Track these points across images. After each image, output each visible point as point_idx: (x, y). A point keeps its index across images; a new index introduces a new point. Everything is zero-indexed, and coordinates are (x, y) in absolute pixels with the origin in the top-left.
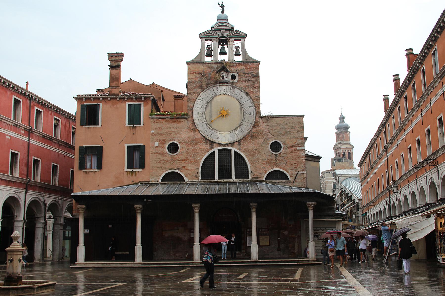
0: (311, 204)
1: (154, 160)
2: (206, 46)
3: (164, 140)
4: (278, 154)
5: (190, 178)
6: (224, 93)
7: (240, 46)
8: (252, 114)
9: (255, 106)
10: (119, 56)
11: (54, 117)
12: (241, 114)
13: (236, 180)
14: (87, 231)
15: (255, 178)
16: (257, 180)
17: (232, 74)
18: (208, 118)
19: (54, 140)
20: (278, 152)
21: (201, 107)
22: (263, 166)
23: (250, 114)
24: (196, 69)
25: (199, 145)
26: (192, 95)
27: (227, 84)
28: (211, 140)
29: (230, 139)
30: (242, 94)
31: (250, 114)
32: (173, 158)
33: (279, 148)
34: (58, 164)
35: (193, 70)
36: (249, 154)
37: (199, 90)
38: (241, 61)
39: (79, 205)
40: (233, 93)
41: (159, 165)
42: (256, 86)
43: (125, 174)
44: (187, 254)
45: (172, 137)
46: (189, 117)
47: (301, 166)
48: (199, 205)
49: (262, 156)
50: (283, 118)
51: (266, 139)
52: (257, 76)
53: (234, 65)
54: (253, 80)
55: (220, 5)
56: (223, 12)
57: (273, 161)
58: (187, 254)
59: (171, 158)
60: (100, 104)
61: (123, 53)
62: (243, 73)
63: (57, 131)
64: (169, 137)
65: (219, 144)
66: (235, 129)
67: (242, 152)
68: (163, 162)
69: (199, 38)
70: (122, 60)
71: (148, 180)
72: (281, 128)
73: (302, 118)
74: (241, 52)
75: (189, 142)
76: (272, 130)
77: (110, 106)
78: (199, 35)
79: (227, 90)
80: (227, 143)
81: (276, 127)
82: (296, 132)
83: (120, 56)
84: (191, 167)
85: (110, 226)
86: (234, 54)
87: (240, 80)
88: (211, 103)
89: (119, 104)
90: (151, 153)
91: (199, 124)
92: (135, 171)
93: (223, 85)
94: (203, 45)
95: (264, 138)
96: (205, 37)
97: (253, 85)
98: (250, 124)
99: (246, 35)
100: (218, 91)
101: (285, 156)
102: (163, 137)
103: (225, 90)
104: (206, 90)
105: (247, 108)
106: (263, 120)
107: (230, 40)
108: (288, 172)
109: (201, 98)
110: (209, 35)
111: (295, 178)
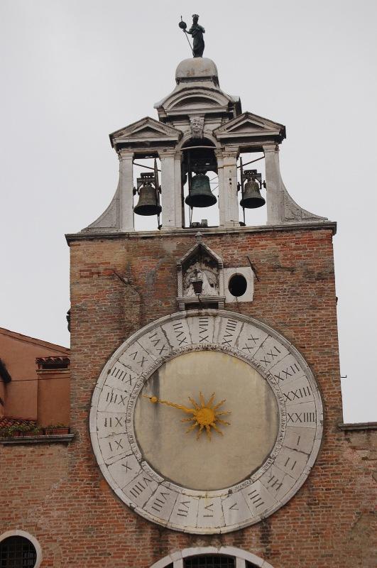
2: (137, 175)
6: (205, 343)
7: (260, 167)
8: (309, 417)
9: (320, 388)
12: (269, 419)
21: (119, 399)
24: (101, 260)
25: (113, 543)
27: (214, 311)
29: (230, 515)
35: (94, 265)
38: (265, 224)
42: (323, 312)
45: (13, 515)
46: (74, 439)
51: (365, 511)
52: (326, 276)
53: (240, 239)
54: (312, 292)
55: (189, 26)
56: (198, 49)
62: (274, 268)
65: (188, 535)
66: (248, 477)
69: (114, 150)
74: (264, 193)
78: (111, 137)
80: (217, 531)
86: (240, 197)
87: (262, 292)
93: (199, 315)
94: (124, 174)
96: (133, 145)
98: (307, 456)
99: (283, 130)
100: (181, 338)
103: (209, 333)
105: (291, 396)
106: (356, 439)
107: (223, 149)
109: (118, 366)
110: (148, 137)
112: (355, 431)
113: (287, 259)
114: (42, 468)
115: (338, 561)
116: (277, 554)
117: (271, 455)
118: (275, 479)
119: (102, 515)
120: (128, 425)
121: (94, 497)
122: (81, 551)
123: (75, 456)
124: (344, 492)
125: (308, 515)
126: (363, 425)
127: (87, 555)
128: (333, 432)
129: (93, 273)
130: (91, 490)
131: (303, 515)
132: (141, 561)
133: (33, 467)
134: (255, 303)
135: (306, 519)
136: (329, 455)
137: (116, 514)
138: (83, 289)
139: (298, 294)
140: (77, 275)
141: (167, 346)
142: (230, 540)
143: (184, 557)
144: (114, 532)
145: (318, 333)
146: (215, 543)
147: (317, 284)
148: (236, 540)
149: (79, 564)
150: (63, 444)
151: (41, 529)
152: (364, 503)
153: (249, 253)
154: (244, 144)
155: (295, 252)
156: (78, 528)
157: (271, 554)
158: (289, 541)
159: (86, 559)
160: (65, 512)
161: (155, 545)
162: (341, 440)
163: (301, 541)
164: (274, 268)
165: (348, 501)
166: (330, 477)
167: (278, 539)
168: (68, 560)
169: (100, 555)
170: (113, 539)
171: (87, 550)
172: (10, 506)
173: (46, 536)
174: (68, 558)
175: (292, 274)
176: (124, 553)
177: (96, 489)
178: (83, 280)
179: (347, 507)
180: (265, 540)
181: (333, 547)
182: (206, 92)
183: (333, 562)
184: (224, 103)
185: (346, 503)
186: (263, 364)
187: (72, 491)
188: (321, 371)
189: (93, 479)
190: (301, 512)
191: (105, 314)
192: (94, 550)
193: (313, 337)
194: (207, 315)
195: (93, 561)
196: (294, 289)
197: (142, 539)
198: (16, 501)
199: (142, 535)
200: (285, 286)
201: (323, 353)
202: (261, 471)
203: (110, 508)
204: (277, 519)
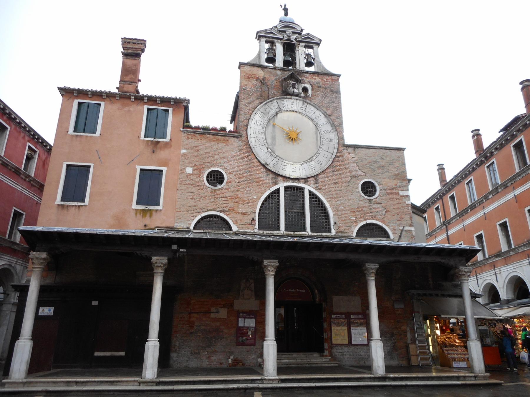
0: (466, 270)
1: (183, 194)
3: (202, 166)
4: (373, 199)
5: (240, 226)
6: (293, 109)
7: (312, 54)
10: (139, 44)
11: (28, 144)
12: (317, 140)
13: (313, 234)
14: (49, 310)
15: (341, 232)
16: (345, 236)
17: (303, 85)
18: (269, 141)
19: (23, 175)
21: (259, 124)
22: (352, 215)
23: (330, 140)
26: (247, 106)
29: (303, 173)
30: (318, 113)
31: (330, 140)
33: (372, 191)
34: (24, 211)
35: (250, 74)
36: (331, 196)
39: (34, 253)
40: (305, 111)
41: (192, 203)
42: (337, 104)
43: (133, 213)
44: (232, 357)
45: (215, 162)
46: (241, 136)
47: (407, 218)
48: (276, 263)
49: (350, 200)
50: (376, 150)
52: (337, 92)
54: (333, 96)
56: (286, 15)
57: (366, 209)
58: (232, 357)
59: (212, 193)
60: (103, 104)
61: (145, 41)
62: (319, 87)
63: (31, 165)
64: (209, 161)
66: (309, 159)
68: (199, 198)
70: (143, 51)
71: (171, 225)
73: (402, 151)
77: (119, 109)
78: (258, 32)
79: (297, 106)
81: (368, 161)
82: (396, 170)
83: (141, 44)
85: (95, 303)
88: (274, 121)
89: (133, 106)
90: (179, 182)
92: (151, 210)
93: (291, 98)
96: (265, 37)
97: (333, 103)
99: (321, 41)
101: (383, 203)
102: (201, 161)
103: (295, 105)
104: (267, 103)
105: (325, 132)
106: (350, 150)
107: (299, 44)
108: (389, 227)
111: (400, 236)
112: (350, 147)
116: (321, 188)
118: (320, 161)
126: (353, 145)
129: (250, 78)
134: (312, 97)
138: (245, 82)
141: (278, 108)
142: (302, 181)
152: (353, 173)
153: (309, 80)
154: (306, 44)
155: (326, 83)
164: (319, 87)
170: (256, 176)
175: (325, 90)
182: (293, 24)
184: (299, 29)
189: (248, 152)
190: (330, 174)
196: (326, 95)
198: (217, 157)
200: (323, 93)
201: (337, 118)
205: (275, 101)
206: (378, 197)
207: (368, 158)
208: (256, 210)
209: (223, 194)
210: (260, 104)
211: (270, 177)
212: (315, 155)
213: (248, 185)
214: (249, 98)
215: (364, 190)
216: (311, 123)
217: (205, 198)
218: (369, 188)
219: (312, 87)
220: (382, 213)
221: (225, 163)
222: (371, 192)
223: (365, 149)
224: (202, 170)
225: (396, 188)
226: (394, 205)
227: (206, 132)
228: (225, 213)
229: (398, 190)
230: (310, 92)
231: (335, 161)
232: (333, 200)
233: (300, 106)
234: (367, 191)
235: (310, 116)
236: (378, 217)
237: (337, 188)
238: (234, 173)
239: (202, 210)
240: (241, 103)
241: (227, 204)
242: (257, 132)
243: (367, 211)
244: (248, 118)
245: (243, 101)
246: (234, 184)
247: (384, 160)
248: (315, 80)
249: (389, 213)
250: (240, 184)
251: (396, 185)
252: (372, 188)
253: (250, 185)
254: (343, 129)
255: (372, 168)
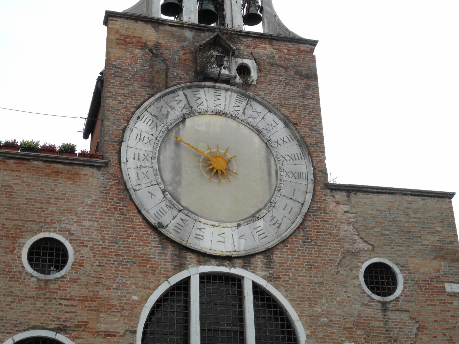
3: (18, 227)
4: (390, 302)
6: (218, 109)
12: (269, 174)
17: (240, 61)
18: (168, 176)
20: (390, 294)
21: (146, 140)
23: (296, 175)
27: (227, 86)
28: (177, 240)
29: (239, 244)
30: (271, 117)
32: (45, 289)
33: (388, 284)
35: (128, 37)
36: (300, 295)
37: (143, 92)
42: (310, 101)
45: (48, 220)
46: (106, 165)
49: (341, 303)
51: (348, 251)
54: (301, 84)
57: (376, 324)
59: (39, 288)
62: (273, 65)
64: (36, 218)
66: (254, 216)
67: (276, 287)
68: (9, 299)
72: (390, 223)
73: (447, 200)
75: (104, 239)
76: (366, 227)
79: (227, 103)
81: (377, 220)
82: (437, 238)
84: (108, 326)
88: (178, 133)
91: (138, 188)
93: (214, 87)
95: (342, 250)
97: (301, 99)
98: (300, 205)
101: (411, 310)
102: (16, 217)
103: (222, 101)
105: (287, 158)
106: (340, 196)
109: (147, 114)
112: (338, 190)
113: (282, 60)
114: (77, 184)
115: (328, 288)
116: (278, 278)
117: (272, 201)
118: (276, 219)
119: (129, 230)
120: (153, 161)
121: (123, 214)
122: (110, 257)
123: (106, 179)
124: (331, 235)
125: (303, 250)
127: (115, 261)
128: (320, 189)
129: (129, 43)
130: (120, 209)
131: (299, 250)
132: (162, 272)
133: (69, 183)
134: (258, 86)
135: (301, 253)
136: (319, 206)
137: (142, 231)
138: (118, 52)
139: (291, 85)
140: (114, 42)
141: (187, 106)
142: (239, 263)
143: (200, 272)
144: (139, 245)
145: (307, 115)
146: (226, 264)
147: (305, 81)
148: (244, 263)
149: (108, 268)
150: (97, 168)
151: (73, 234)
152: (347, 246)
153: (252, 50)
155: (287, 56)
156: (107, 238)
157: (274, 278)
158: (288, 269)
159: (114, 264)
160: (96, 223)
161: (176, 260)
162: (328, 195)
163: (298, 270)
164: (273, 65)
165: (335, 242)
166: (320, 223)
167: (280, 266)
168: (97, 263)
169: (128, 262)
170: (139, 251)
171: (114, 257)
172: (46, 212)
173: (78, 241)
174: (97, 262)
175: (286, 71)
176: (148, 264)
177: (125, 208)
178: (118, 46)
179: (334, 247)
180: (268, 266)
181: (323, 277)
183: (324, 289)
185: (333, 244)
186: (265, 131)
187: (103, 207)
188: (310, 143)
189: (121, 199)
190: (297, 247)
191: (136, 74)
192: (121, 258)
193: (303, 118)
194: (220, 88)
195: (120, 267)
196: (288, 81)
197: (164, 253)
199: (164, 250)
200: (281, 78)
201: (311, 129)
202: (264, 212)
203: (136, 224)
204: (278, 251)
205: (181, 93)
206: (402, 298)
207: (378, 213)
208: (136, 327)
209: (63, 290)
210: (149, 98)
211: (169, 254)
212: (265, 206)
213: (120, 271)
214: (126, 85)
215: (372, 283)
216: (256, 139)
217: (24, 300)
218: (382, 278)
219: (258, 64)
220: (410, 332)
221: (71, 223)
222: (386, 286)
223: (371, 195)
224: (19, 238)
225: (438, 277)
226: (435, 314)
227: (30, 156)
228: (69, 333)
229: (443, 282)
230: (254, 74)
231: (309, 219)
232: (306, 303)
233: (233, 104)
234: (377, 283)
235: (254, 125)
236: (403, 340)
237: (315, 277)
238: (91, 244)
239: (15, 326)
240: (108, 94)
241: (72, 312)
242: (142, 157)
243: (378, 327)
244: (122, 126)
245: (112, 90)
246: (89, 269)
247: (411, 217)
248: (265, 52)
249: (425, 331)
250: (102, 269)
251: (438, 271)
252: (388, 278)
253: (124, 271)
254: (323, 152)
255: (387, 235)
